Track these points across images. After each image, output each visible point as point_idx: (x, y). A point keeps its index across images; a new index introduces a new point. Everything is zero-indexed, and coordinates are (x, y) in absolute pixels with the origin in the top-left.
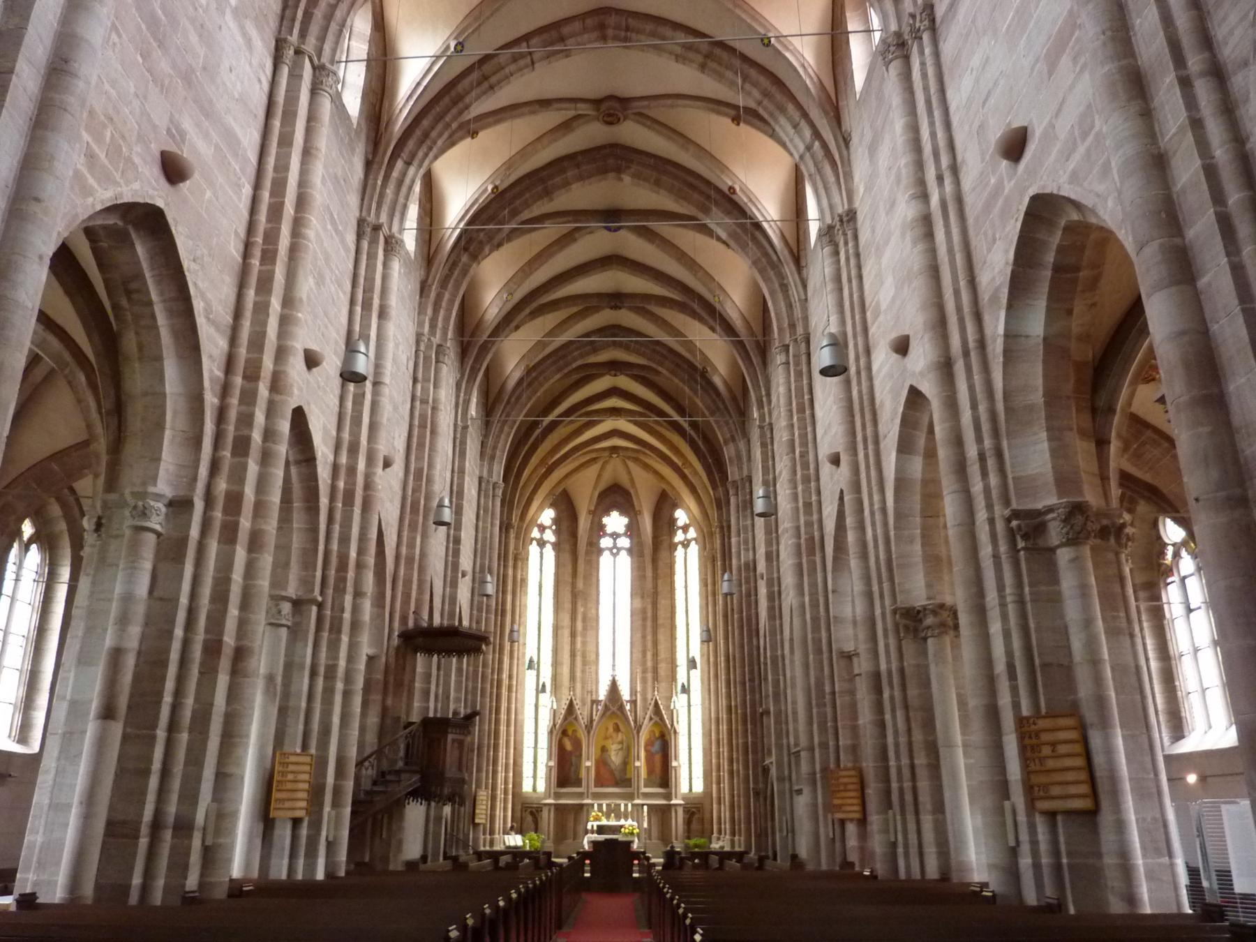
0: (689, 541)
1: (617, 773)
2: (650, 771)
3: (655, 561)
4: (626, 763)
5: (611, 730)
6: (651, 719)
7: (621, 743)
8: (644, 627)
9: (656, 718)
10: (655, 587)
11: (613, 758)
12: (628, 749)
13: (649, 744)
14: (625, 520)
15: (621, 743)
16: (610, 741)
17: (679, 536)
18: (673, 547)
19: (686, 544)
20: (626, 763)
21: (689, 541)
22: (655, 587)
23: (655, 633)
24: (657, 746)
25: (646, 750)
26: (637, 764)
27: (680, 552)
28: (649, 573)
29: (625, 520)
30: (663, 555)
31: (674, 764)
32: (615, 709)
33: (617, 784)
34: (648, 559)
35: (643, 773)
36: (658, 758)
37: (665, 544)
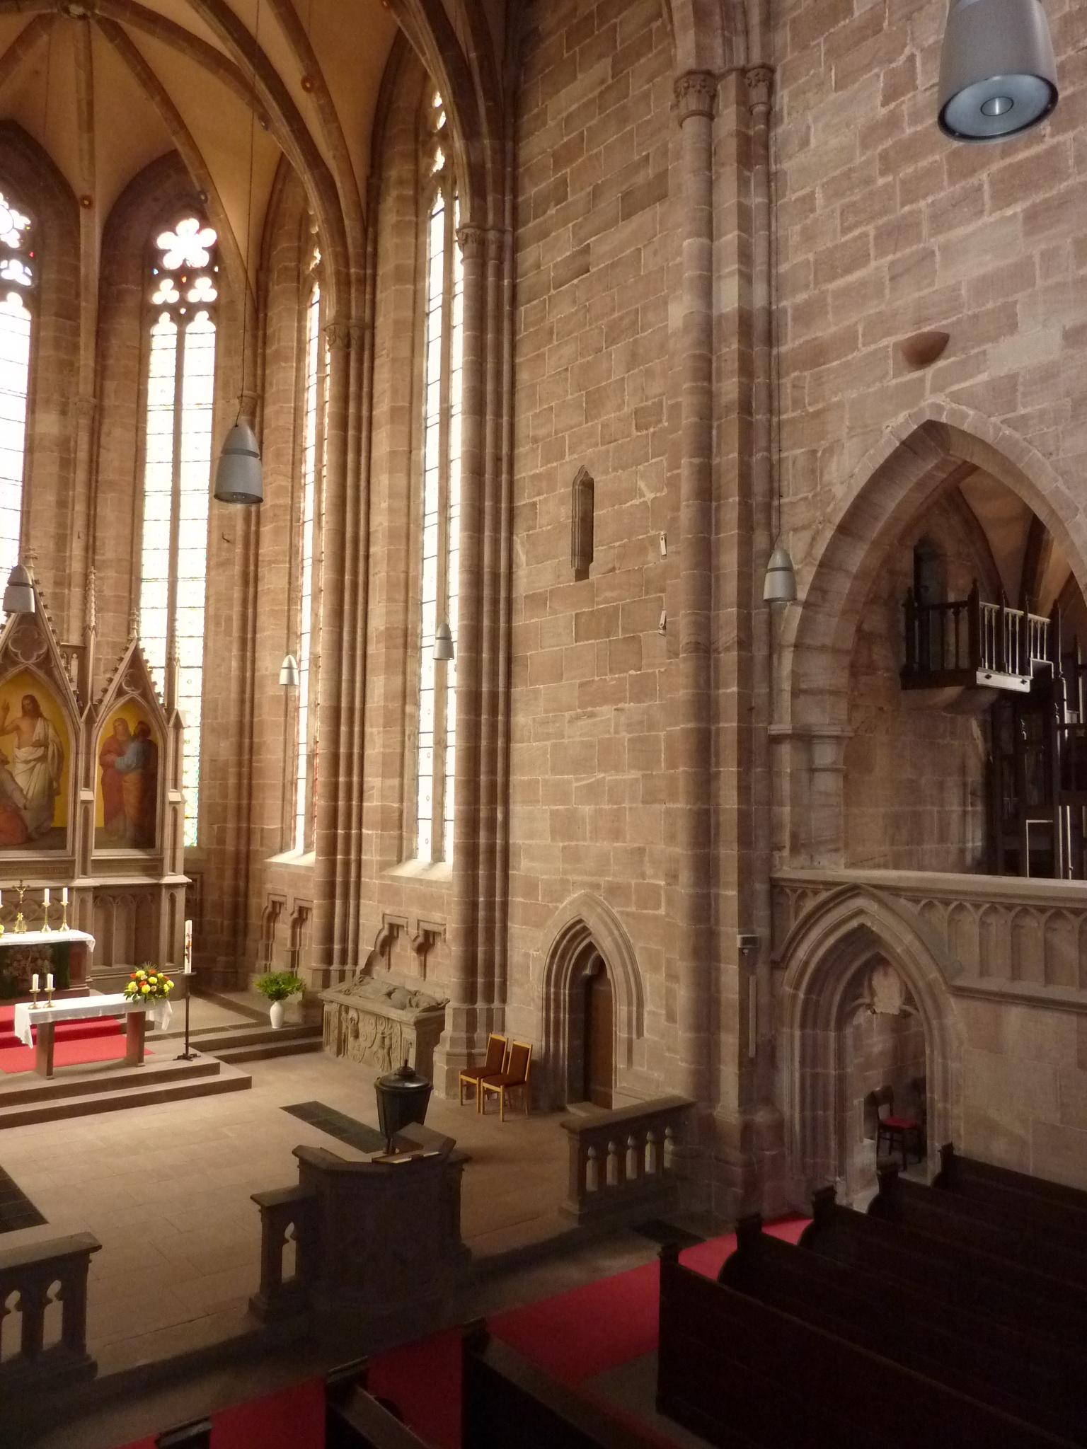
0: (193, 309)
1: (27, 816)
2: (112, 811)
3: (101, 336)
4: (52, 791)
5: (16, 712)
6: (120, 693)
7: (43, 744)
8: (65, 484)
9: (132, 693)
10: (99, 393)
11: (21, 780)
12: (61, 757)
13: (113, 748)
14: (23, 222)
15: (38, 744)
16: (13, 738)
17: (165, 293)
18: (149, 314)
19: (182, 314)
20: (52, 791)
21: (193, 309)
22: (99, 393)
23: (91, 502)
24: (132, 750)
25: (102, 764)
26: (85, 795)
27: (164, 329)
28: (86, 358)
29: (23, 222)
30: (125, 324)
31: (172, 796)
32: (25, 663)
33: (28, 842)
34: (87, 323)
35: (97, 819)
36: (131, 782)
37: (131, 303)
